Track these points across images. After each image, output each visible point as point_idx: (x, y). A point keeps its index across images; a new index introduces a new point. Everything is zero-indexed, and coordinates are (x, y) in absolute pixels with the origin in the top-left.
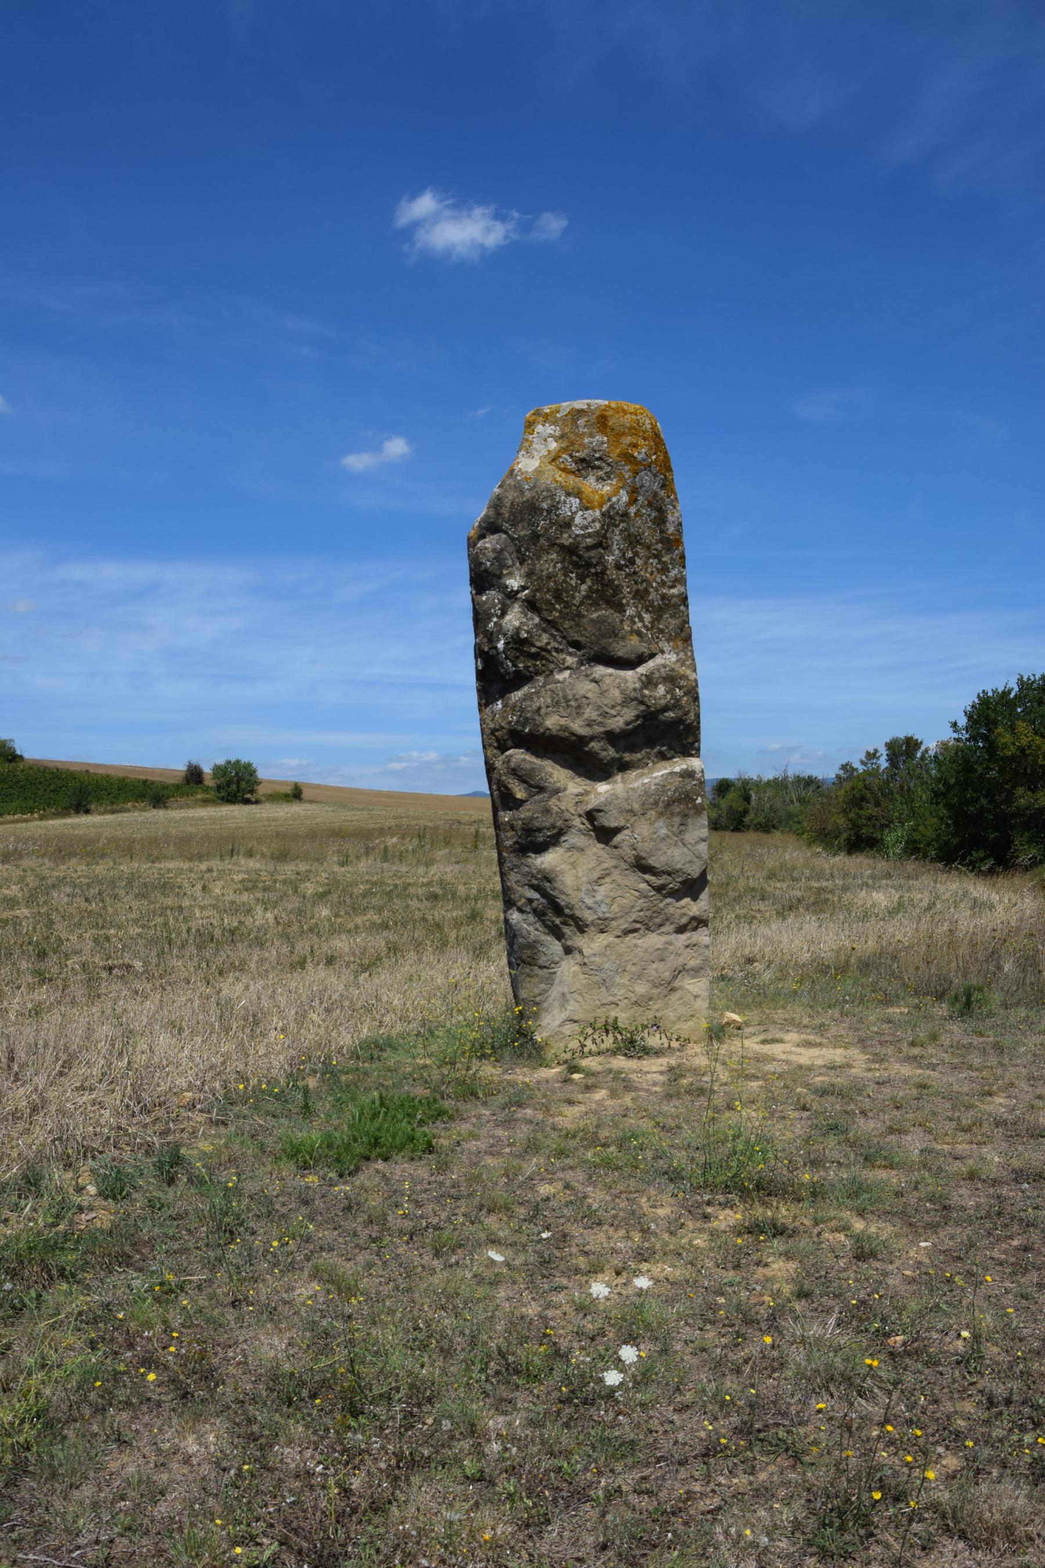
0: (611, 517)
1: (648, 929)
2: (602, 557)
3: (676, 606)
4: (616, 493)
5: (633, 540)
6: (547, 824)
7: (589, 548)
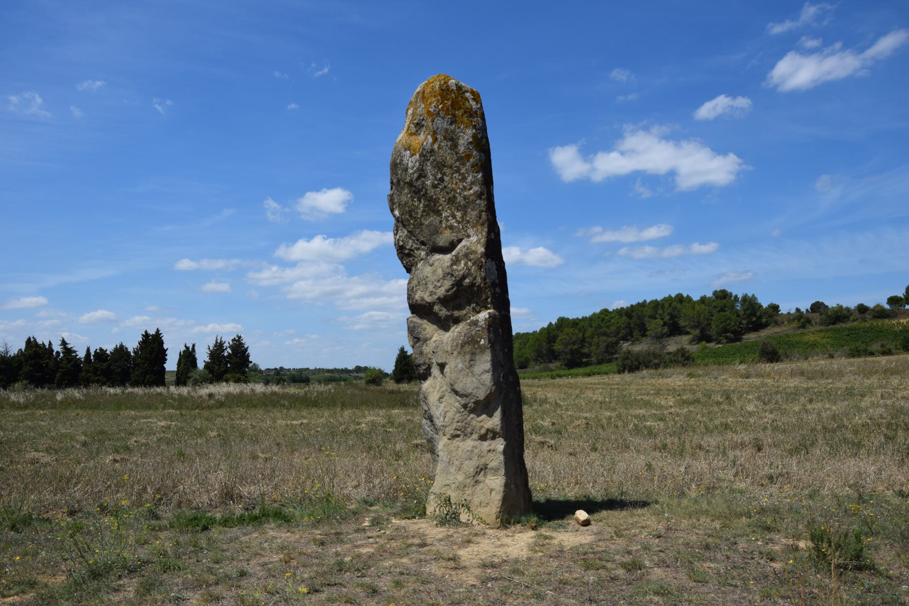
0: (424, 156)
1: (466, 435)
2: (423, 183)
3: (474, 202)
4: (426, 138)
5: (440, 166)
6: (422, 362)
7: (417, 179)
